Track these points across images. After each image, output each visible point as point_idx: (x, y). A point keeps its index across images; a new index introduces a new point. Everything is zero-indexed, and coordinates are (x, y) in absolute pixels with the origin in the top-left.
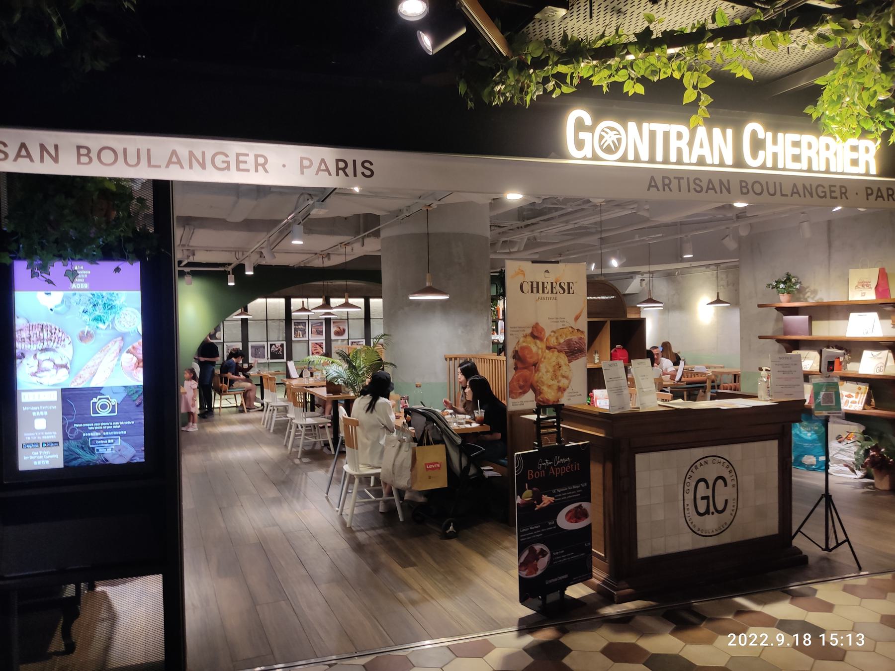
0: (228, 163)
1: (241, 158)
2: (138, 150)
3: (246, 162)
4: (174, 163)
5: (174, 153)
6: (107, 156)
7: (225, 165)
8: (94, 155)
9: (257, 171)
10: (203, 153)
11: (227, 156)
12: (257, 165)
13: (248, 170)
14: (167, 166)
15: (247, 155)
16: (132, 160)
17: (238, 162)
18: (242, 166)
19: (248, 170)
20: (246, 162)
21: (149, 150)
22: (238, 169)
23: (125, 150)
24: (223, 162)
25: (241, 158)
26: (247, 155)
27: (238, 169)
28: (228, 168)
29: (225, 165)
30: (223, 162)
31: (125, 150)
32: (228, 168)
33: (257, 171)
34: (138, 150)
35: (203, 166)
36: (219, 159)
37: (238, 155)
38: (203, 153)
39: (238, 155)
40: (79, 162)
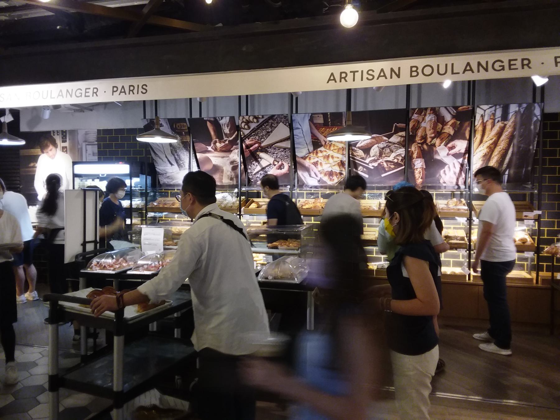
0: (503, 66)
1: (512, 62)
2: (446, 65)
3: (515, 65)
4: (382, 76)
5: (468, 64)
6: (428, 71)
7: (501, 68)
8: (420, 71)
9: (523, 68)
10: (487, 62)
11: (502, 62)
12: (523, 65)
13: (517, 69)
14: (464, 73)
15: (516, 60)
16: (442, 71)
17: (510, 65)
18: (512, 67)
19: (517, 69)
20: (515, 65)
21: (453, 64)
22: (510, 69)
23: (438, 65)
24: (500, 66)
25: (512, 62)
26: (516, 60)
27: (510, 69)
28: (503, 69)
29: (501, 68)
30: (500, 66)
31: (438, 65)
32: (503, 69)
33: (523, 68)
34: (446, 65)
35: (486, 70)
36: (497, 66)
37: (510, 61)
38: (487, 62)
39: (510, 61)
40: (411, 76)
